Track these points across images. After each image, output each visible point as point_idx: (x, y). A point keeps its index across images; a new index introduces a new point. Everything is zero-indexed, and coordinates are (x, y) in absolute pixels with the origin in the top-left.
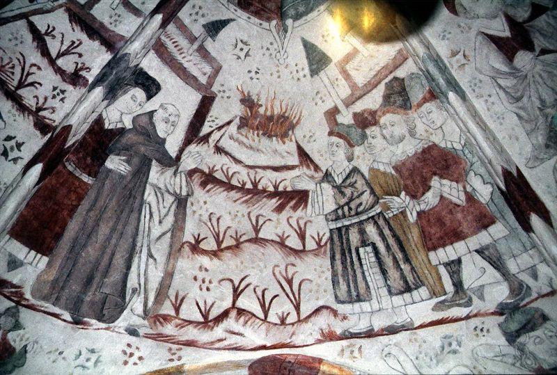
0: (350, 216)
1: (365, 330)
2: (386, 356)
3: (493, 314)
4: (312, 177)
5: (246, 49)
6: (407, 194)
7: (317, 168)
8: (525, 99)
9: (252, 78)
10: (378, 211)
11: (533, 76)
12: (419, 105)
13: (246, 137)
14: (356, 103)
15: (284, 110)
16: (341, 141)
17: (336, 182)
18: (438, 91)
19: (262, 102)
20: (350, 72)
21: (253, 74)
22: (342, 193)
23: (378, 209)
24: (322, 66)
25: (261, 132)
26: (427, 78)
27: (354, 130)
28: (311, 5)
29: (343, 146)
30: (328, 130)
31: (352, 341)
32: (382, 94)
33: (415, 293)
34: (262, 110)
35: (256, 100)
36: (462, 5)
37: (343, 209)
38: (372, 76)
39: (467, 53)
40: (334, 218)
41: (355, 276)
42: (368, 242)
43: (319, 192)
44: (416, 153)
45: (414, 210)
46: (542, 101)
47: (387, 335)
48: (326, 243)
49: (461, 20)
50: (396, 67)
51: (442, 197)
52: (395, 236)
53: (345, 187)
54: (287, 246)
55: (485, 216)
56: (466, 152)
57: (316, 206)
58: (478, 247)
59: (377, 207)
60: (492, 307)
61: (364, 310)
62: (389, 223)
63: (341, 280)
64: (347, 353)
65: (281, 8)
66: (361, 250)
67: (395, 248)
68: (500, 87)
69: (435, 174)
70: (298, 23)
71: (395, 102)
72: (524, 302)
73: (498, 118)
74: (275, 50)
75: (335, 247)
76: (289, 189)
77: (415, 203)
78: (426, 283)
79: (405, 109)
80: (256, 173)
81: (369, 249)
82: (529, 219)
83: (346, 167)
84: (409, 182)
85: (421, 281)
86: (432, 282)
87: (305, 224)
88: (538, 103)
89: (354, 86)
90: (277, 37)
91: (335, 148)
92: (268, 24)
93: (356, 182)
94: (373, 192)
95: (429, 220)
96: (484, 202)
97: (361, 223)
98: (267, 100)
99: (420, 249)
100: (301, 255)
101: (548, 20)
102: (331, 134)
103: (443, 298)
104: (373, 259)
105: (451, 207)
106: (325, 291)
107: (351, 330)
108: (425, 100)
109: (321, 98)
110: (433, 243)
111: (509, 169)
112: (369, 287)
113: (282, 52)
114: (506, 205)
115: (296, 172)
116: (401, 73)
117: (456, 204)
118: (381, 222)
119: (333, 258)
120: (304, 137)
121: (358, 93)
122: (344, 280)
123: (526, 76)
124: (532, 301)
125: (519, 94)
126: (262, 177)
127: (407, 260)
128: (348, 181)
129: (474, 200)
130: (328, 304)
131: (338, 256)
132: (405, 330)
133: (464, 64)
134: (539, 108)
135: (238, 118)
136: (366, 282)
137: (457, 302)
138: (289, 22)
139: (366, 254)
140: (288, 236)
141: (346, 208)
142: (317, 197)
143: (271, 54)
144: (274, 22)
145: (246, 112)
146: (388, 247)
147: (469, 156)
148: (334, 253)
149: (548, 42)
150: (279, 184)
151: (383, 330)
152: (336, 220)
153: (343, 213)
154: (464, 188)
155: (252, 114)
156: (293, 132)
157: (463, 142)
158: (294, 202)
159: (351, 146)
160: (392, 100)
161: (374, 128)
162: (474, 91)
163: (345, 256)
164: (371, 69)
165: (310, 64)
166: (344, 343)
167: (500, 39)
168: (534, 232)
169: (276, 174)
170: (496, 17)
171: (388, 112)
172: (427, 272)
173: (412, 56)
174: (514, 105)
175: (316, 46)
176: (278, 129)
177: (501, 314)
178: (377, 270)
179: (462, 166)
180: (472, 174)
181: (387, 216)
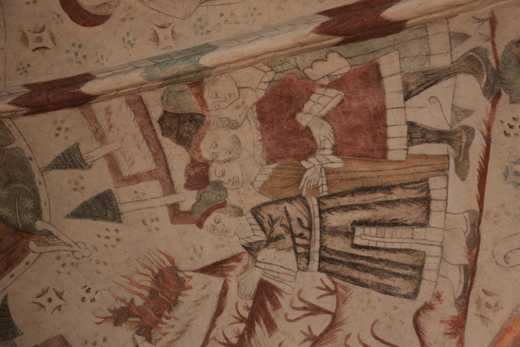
0: (310, 238)
1: (463, 276)
2: (506, 262)
3: (494, 106)
4: (246, 268)
5: (51, 294)
6: (306, 158)
7: (236, 258)
9: (93, 300)
10: (315, 202)
12: (203, 104)
13: (165, 334)
14: (173, 180)
15: (150, 273)
16: (214, 215)
17: (262, 241)
18: (193, 75)
19: (128, 297)
20: (133, 173)
21: (88, 296)
22: (278, 238)
23: (313, 202)
24: (112, 205)
25: (166, 313)
26: (174, 83)
27: (205, 194)
28: (29, 190)
29: (220, 214)
30: (195, 226)
31: (472, 299)
32: (174, 144)
33: (434, 194)
34: (139, 302)
35: (123, 305)
36: (100, 5)
37: (298, 245)
38: (147, 148)
39: (159, 24)
40: (305, 260)
41: (388, 262)
42: (350, 230)
43: (268, 267)
44: (261, 130)
45: (328, 157)
47: (478, 250)
48: (334, 283)
49: (117, 14)
50: (147, 115)
51: (324, 118)
52: (353, 193)
53: (272, 231)
54: (322, 335)
55: (366, 74)
56: (279, 68)
57: (282, 276)
58: (401, 97)
59: (309, 202)
60: (485, 104)
61: (435, 266)
62: (334, 195)
63: (387, 282)
64: (489, 313)
65: (16, 230)
66: (357, 241)
67: (368, 198)
69: (293, 116)
70: (45, 215)
71: (189, 132)
72: (493, 61)
74: (68, 256)
75: (342, 273)
76: (250, 303)
77: (321, 152)
78: (425, 175)
79: (202, 122)
80: (215, 340)
81: (359, 231)
82: (387, 21)
83: (248, 219)
84: (292, 151)
85: (421, 182)
86: (427, 168)
87: (301, 299)
89: (151, 175)
90: (56, 248)
91: (220, 227)
92: (31, 254)
93: (270, 216)
94: (290, 200)
95: (347, 143)
96: (347, 69)
97: (322, 228)
98: (127, 290)
99: (380, 167)
100: (339, 319)
102: (200, 225)
103: (452, 161)
104: (373, 230)
105: (340, 110)
106: (396, 308)
107: (458, 294)
108: (200, 95)
109: (152, 221)
110: (378, 149)
111: (318, 24)
112: (408, 250)
113: (75, 248)
114: (360, 43)
115: (232, 286)
116: (156, 113)
117: (339, 105)
118: (330, 203)
119: (356, 282)
120: (192, 259)
121: (164, 174)
122: (388, 277)
124: (495, 50)
126: (223, 332)
127: (388, 188)
128: (266, 225)
129: (341, 79)
130: (413, 312)
131: (356, 274)
132: (479, 223)
133: (173, 32)
135: (136, 336)
136: (400, 250)
137: (463, 145)
138: (40, 225)
139: (364, 237)
140: (309, 328)
141: (298, 241)
142: (272, 271)
143: (73, 264)
144: (32, 245)
145: (132, 322)
146: (365, 207)
147: (286, 67)
148: (349, 277)
150: (239, 314)
151: (470, 253)
152: (308, 258)
153: (303, 246)
154: (322, 86)
155: (137, 316)
156: (182, 271)
157: (266, 69)
158: (268, 303)
159: (223, 205)
160: (185, 135)
161: (212, 170)
162: (208, 32)
163: (359, 264)
164: (139, 146)
165: (105, 218)
166: (472, 310)
168: (406, 21)
169: (225, 314)
171: (198, 145)
172: (411, 170)
173: (140, 90)
175: (85, 202)
176: (171, 289)
177: (498, 95)
178: (389, 230)
179: (295, 81)
180: (308, 71)
181: (326, 194)
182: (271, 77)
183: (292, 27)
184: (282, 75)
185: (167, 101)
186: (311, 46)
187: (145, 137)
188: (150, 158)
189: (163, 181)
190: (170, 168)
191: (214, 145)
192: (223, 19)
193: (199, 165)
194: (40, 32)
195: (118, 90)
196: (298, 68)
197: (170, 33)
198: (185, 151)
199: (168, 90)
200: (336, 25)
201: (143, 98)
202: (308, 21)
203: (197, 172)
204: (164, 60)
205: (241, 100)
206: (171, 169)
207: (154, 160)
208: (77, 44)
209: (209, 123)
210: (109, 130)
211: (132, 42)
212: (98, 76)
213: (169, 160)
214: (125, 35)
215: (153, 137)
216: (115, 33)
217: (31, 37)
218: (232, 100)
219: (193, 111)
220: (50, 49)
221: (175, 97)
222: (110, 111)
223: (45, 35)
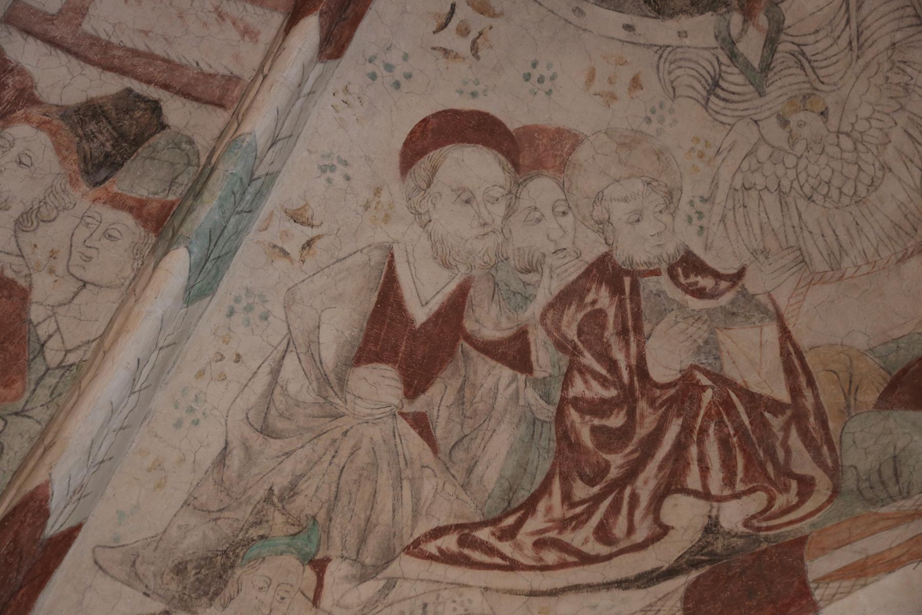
8: (276, 445)
11: (345, 433)
12: (117, 202)
14: (31, 40)
32: (94, 93)
36: (434, 174)
39: (318, 244)
46: (292, 490)
56: (50, 381)
68: (275, 372)
71: (90, 137)
73: (191, 410)
79: (87, 173)
88: (280, 482)
101: (501, 387)
108: (137, 209)
111: (54, 504)
121: (59, 31)
123: (337, 416)
125: (280, 424)
133: (285, 254)
134: (271, 489)
147: (43, 394)
149: (449, 420)
157: (72, 358)
160: (92, 127)
162: (231, 313)
164: (146, 33)
167: (400, 306)
170: (446, 265)
171: (53, 134)
173: (235, 114)
174: (247, 431)
182: (49, 354)
183: (99, 459)
184: (34, 377)
185: (177, 146)
186: (30, 466)
187: (151, 57)
188: (107, 34)
189: (46, 20)
190: (59, 52)
191: (25, 160)
192: (229, 355)
193: (15, 105)
194: (474, 42)
195: (265, 77)
196: (17, 414)
197: (288, 250)
198: (64, 103)
199: (195, 161)
200: (17, 533)
201: (220, 111)
202: (79, 493)
203: (5, 89)
204: (248, 197)
205: (60, 269)
206: (53, 52)
207: (98, 39)
208: (403, 81)
209: (73, 183)
210: (216, 9)
211: (328, 174)
212: (320, 66)
213: (74, 61)
214: (349, 172)
215: (140, 70)
216: (368, 159)
217: (478, 22)
218: (76, 256)
219: (121, 174)
220: (434, 32)
221: (172, 164)
222: (247, 38)
223: (463, 46)
